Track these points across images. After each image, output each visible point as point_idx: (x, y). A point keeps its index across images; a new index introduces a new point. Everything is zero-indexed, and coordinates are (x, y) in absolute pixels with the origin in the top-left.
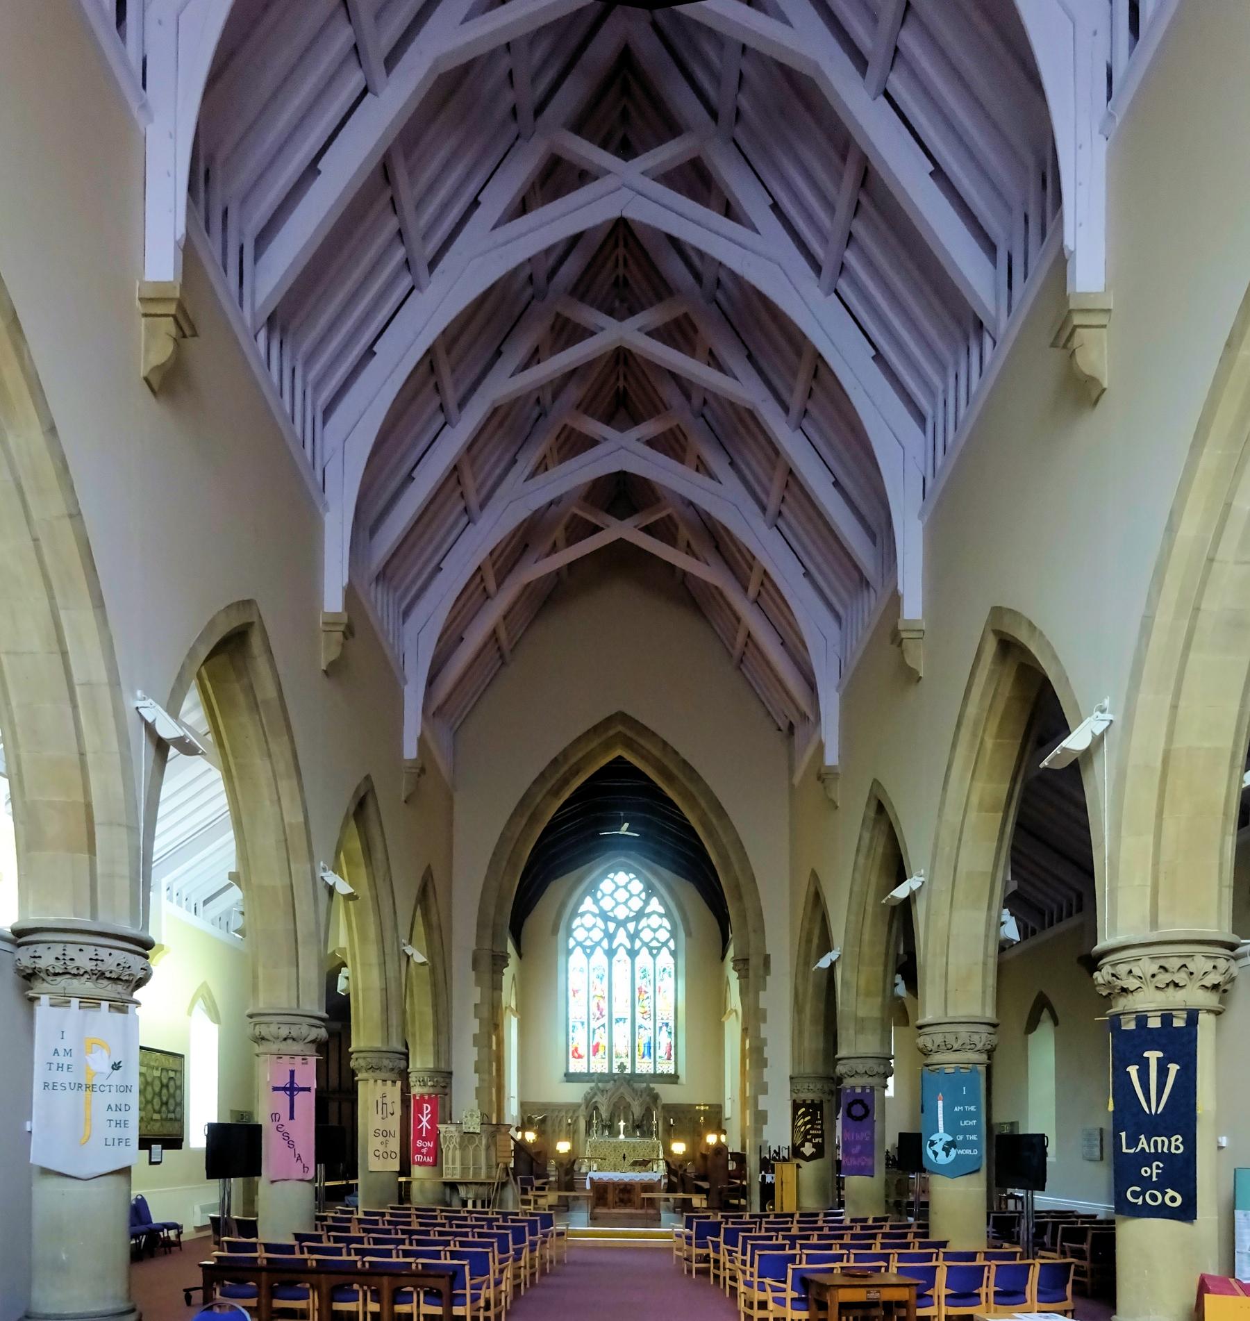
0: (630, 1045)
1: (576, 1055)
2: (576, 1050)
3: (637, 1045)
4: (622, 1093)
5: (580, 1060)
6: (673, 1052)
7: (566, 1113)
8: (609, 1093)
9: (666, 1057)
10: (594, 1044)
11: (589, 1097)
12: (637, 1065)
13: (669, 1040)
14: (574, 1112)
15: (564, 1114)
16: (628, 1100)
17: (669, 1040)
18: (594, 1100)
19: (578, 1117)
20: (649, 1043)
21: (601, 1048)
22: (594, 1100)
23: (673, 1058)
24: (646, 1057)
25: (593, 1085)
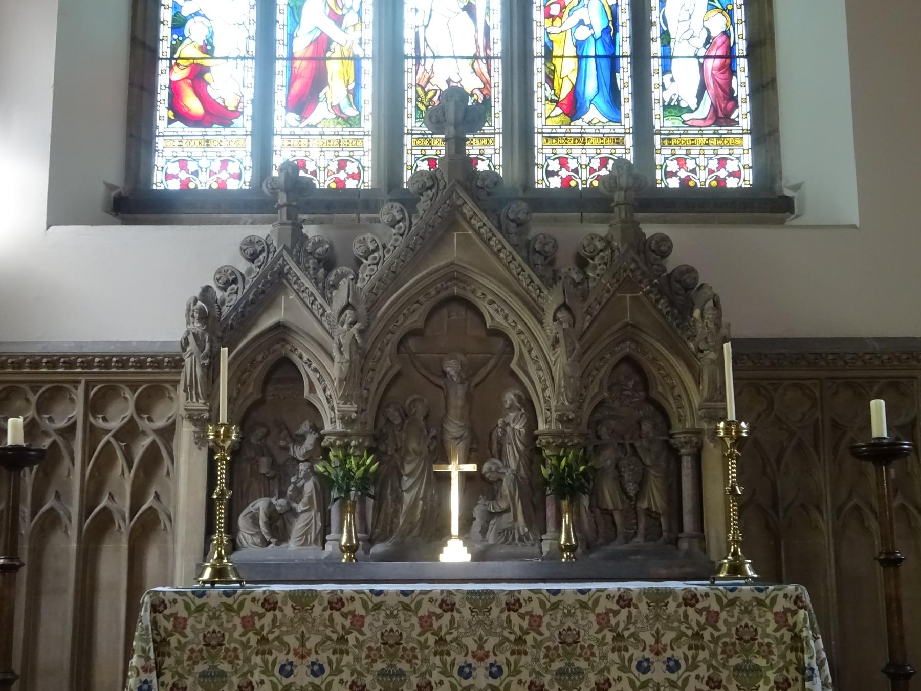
0: (497, 49)
1: (193, 104)
2: (197, 75)
3: (538, 48)
4: (454, 274)
5: (215, 129)
6: (741, 84)
7: (95, 406)
8: (368, 275)
9: (705, 110)
10: (301, 46)
11: (230, 300)
12: (542, 152)
13: (718, 24)
14: (143, 407)
15: (78, 411)
16: (494, 316)
17: (718, 24)
18: (267, 322)
19: (168, 433)
20: (609, 35)
21: (336, 71)
22: (267, 322)
23: (743, 112)
24: (594, 114)
25: (262, 231)
